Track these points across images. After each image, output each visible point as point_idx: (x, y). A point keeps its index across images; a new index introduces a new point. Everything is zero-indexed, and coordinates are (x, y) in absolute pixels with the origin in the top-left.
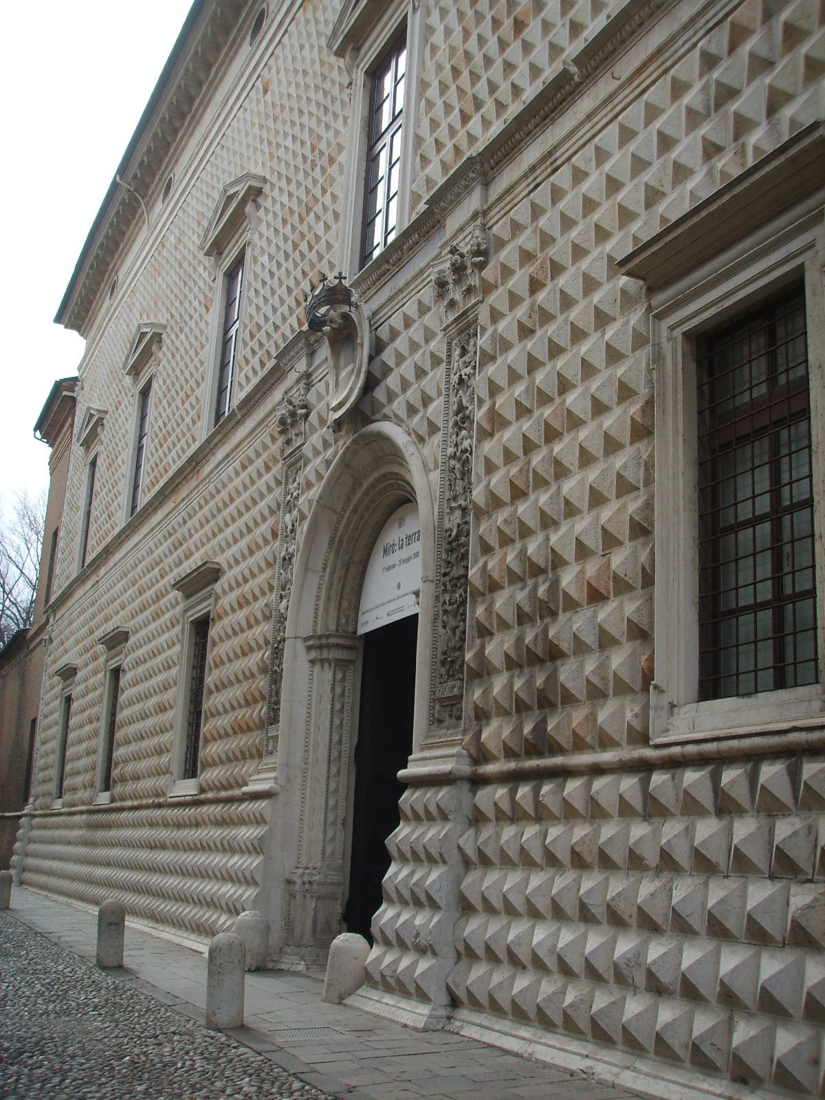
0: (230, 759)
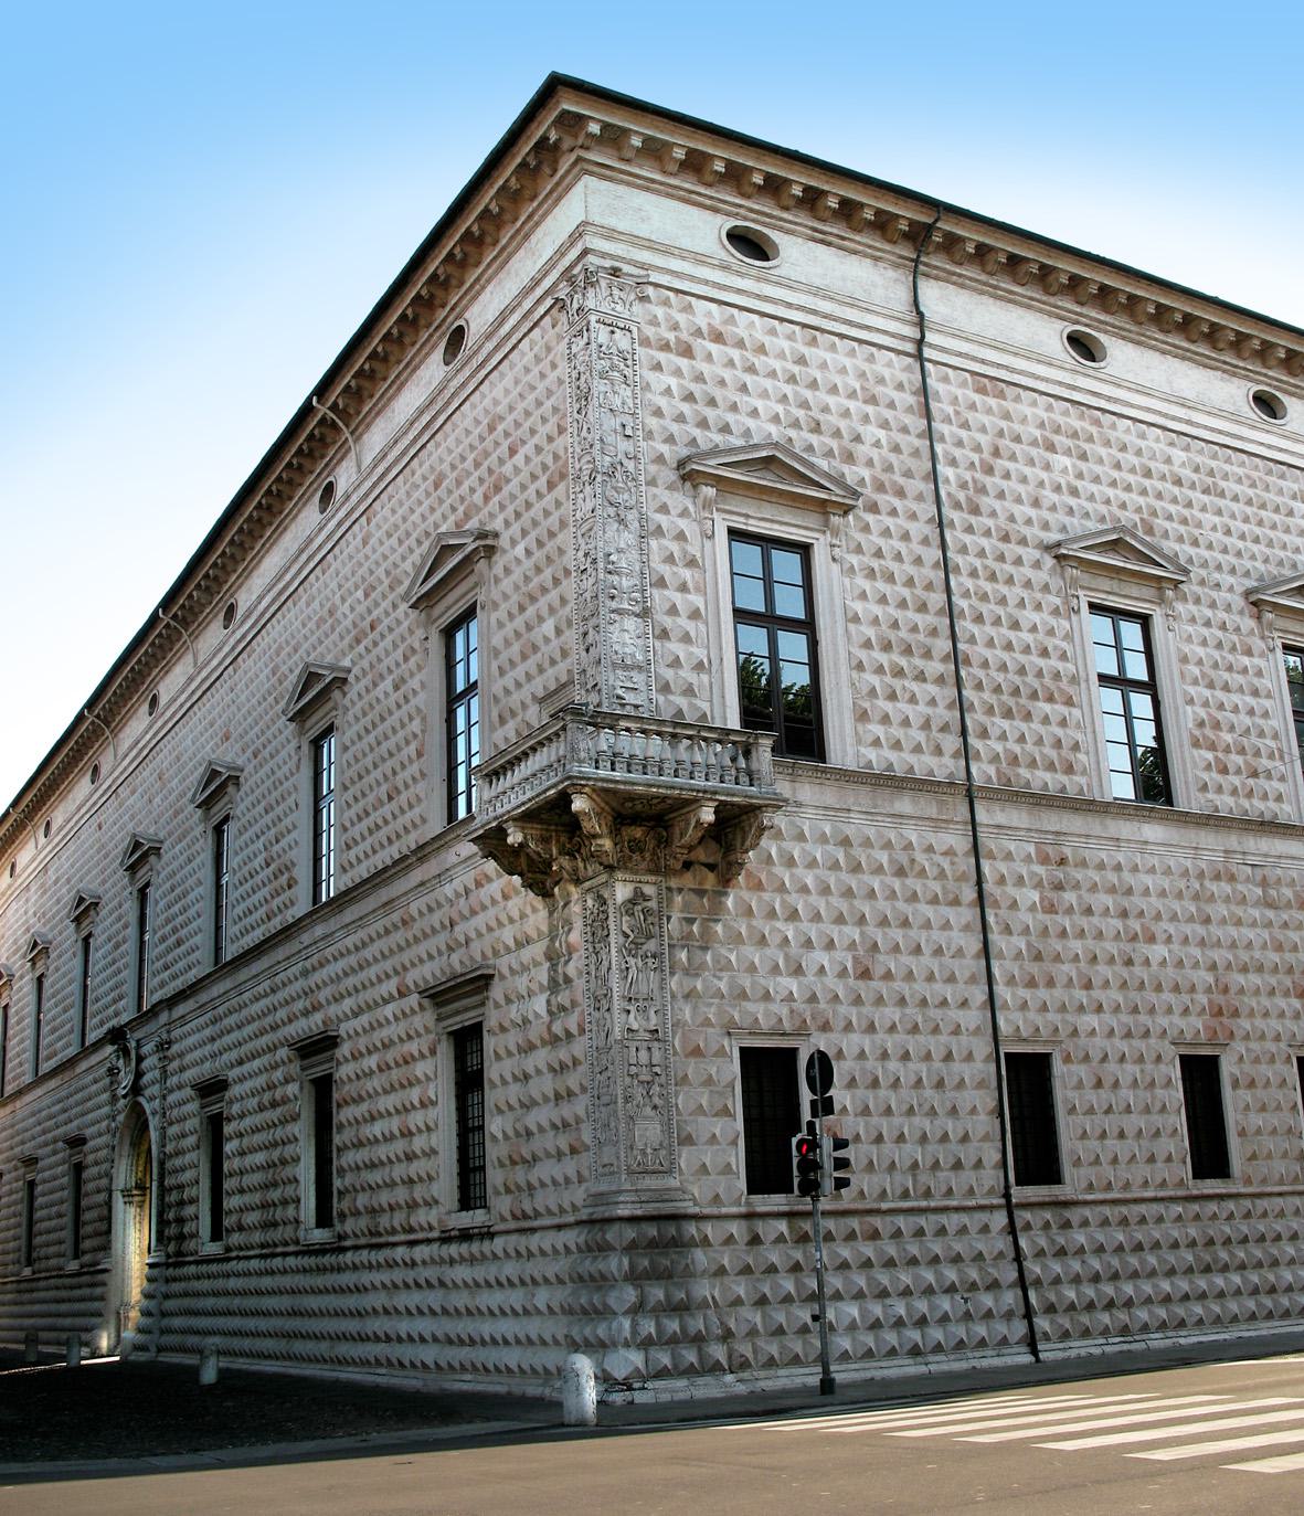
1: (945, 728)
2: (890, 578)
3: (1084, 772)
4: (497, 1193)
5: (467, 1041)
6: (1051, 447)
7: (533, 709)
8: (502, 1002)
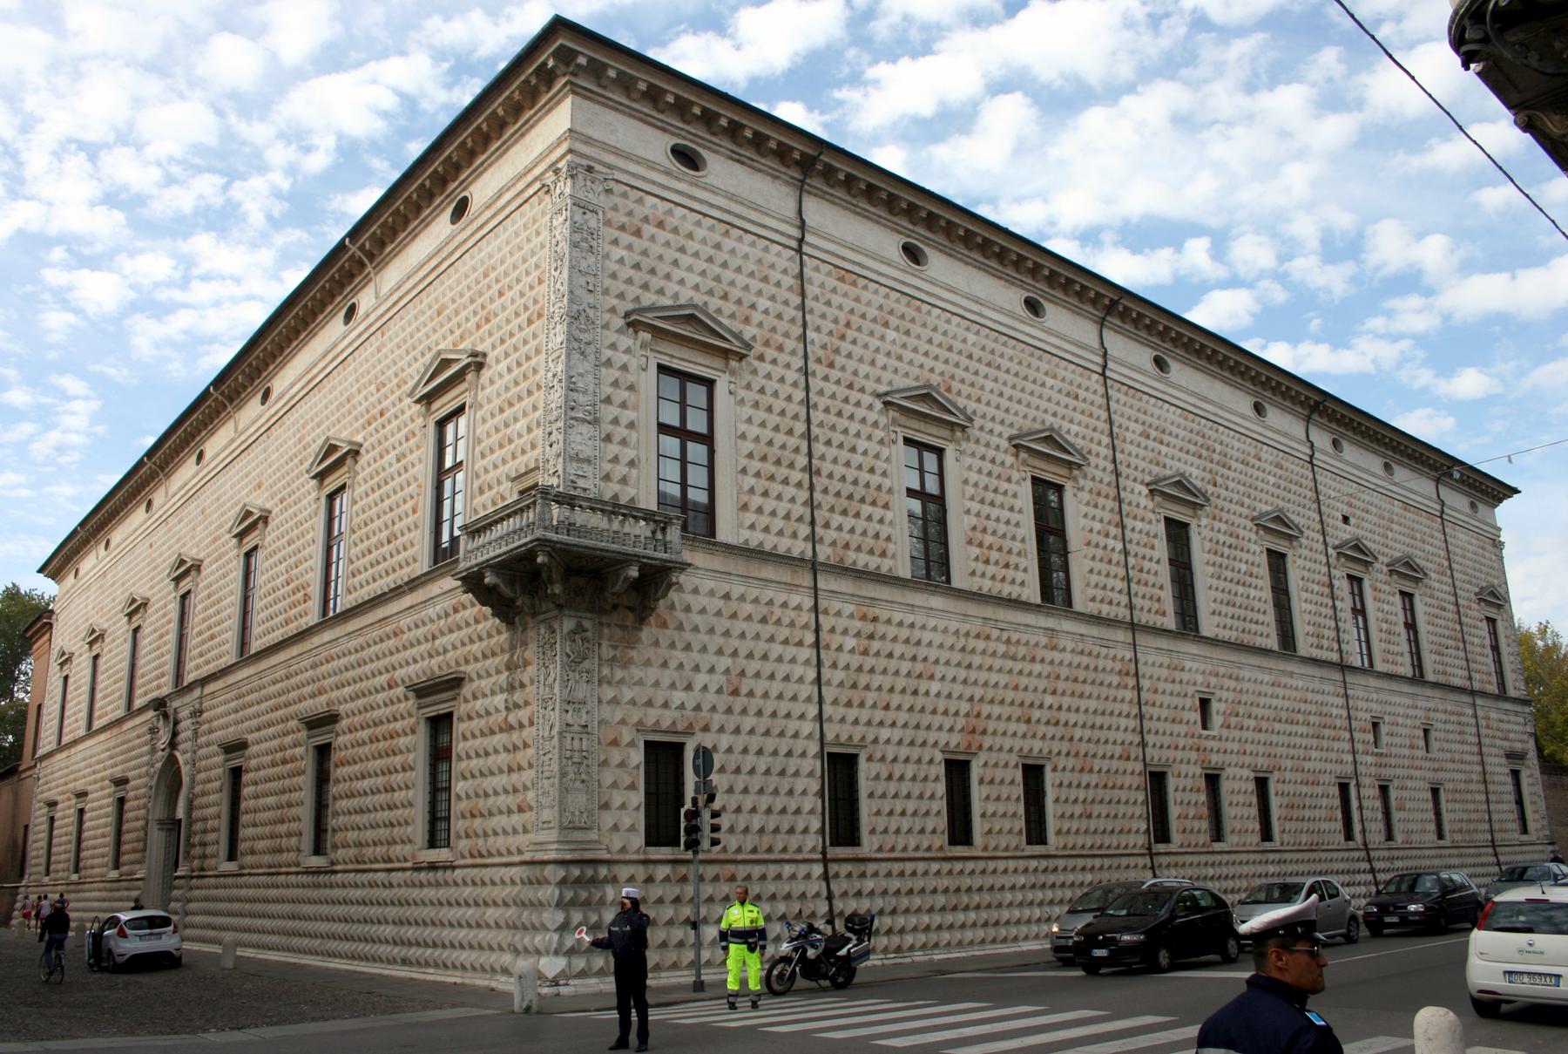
0: (132, 863)
1: (800, 519)
2: (769, 409)
3: (893, 557)
4: (459, 837)
5: (440, 725)
6: (886, 325)
7: (507, 485)
8: (470, 697)
